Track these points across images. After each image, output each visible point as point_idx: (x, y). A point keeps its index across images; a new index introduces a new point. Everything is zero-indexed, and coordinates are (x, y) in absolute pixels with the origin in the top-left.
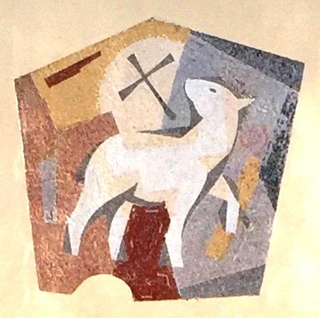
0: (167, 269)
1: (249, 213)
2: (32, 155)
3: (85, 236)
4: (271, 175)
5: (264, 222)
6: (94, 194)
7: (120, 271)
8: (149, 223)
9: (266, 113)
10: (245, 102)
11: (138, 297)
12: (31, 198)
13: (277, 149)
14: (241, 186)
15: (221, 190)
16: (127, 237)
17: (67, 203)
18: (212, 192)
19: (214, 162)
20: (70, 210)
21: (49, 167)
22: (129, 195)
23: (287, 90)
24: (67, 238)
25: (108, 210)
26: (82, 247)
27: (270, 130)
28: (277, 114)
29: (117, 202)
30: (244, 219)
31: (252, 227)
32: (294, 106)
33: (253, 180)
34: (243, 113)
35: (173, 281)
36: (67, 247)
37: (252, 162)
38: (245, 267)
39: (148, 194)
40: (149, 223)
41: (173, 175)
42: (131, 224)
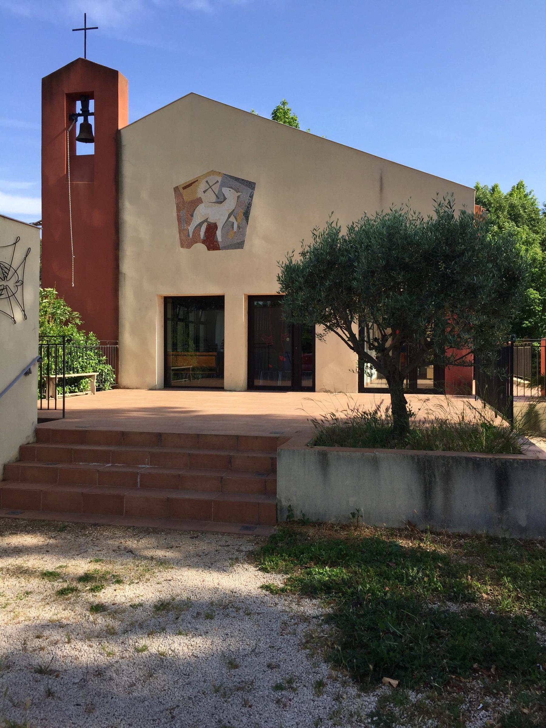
0: (217, 242)
1: (240, 226)
2: (179, 209)
3: (194, 232)
4: (247, 215)
5: (244, 228)
6: (197, 219)
7: (204, 242)
8: (212, 228)
9: (245, 197)
10: (239, 194)
11: (209, 249)
12: (178, 221)
13: (248, 207)
14: (238, 218)
15: (232, 219)
16: (206, 232)
17: (188, 223)
18: (229, 220)
19: (230, 211)
20: (189, 225)
21: (183, 213)
22: (206, 220)
23: (251, 190)
24: (189, 233)
25: (200, 225)
26: (193, 235)
27: (246, 202)
28: (248, 197)
29: (203, 222)
30: (239, 227)
31: (241, 230)
32: (253, 195)
33: (241, 216)
34: (238, 197)
35: (219, 245)
36: (189, 236)
37: (241, 211)
38: (239, 241)
39: (211, 220)
40: (212, 228)
41: (218, 214)
42: (207, 229)
